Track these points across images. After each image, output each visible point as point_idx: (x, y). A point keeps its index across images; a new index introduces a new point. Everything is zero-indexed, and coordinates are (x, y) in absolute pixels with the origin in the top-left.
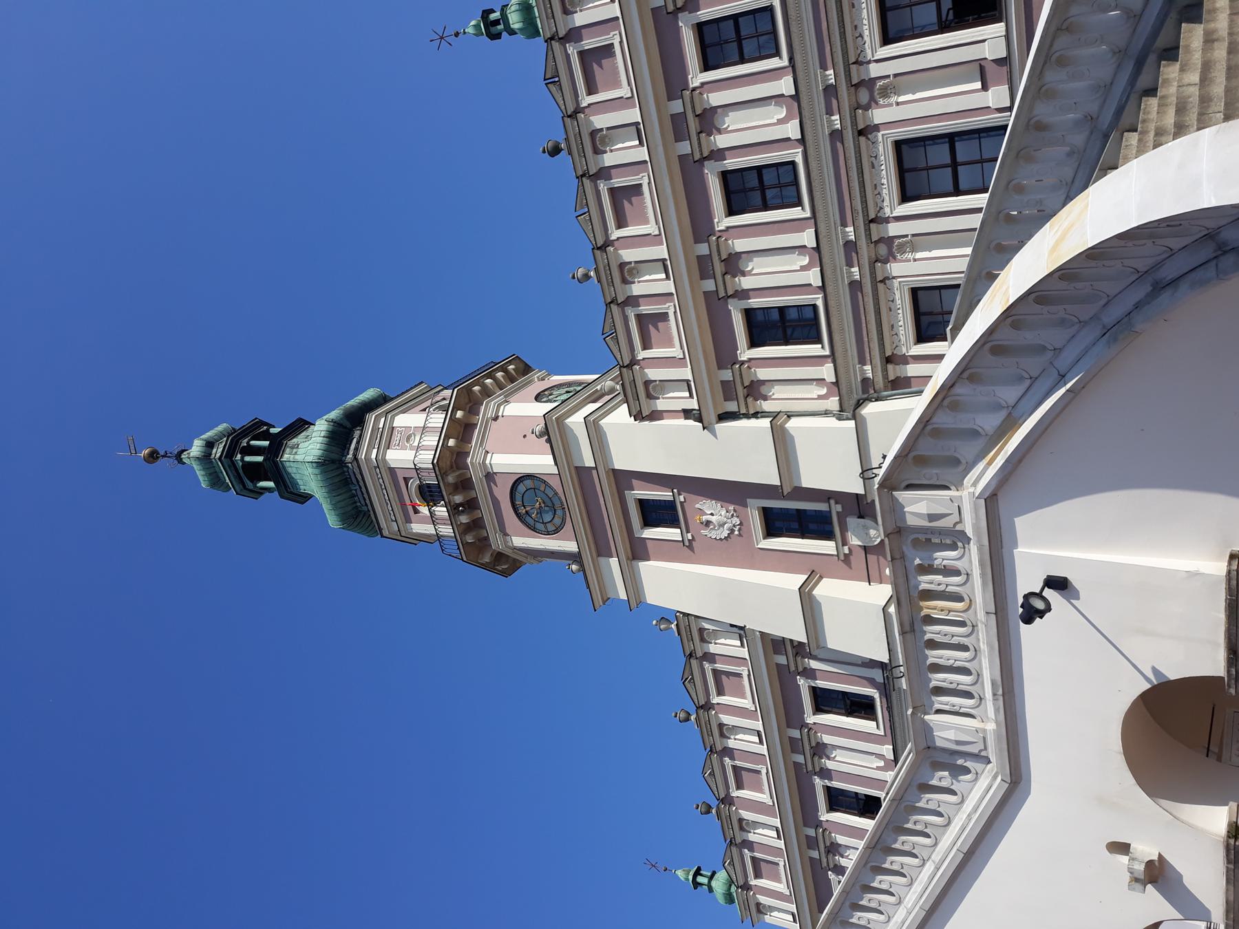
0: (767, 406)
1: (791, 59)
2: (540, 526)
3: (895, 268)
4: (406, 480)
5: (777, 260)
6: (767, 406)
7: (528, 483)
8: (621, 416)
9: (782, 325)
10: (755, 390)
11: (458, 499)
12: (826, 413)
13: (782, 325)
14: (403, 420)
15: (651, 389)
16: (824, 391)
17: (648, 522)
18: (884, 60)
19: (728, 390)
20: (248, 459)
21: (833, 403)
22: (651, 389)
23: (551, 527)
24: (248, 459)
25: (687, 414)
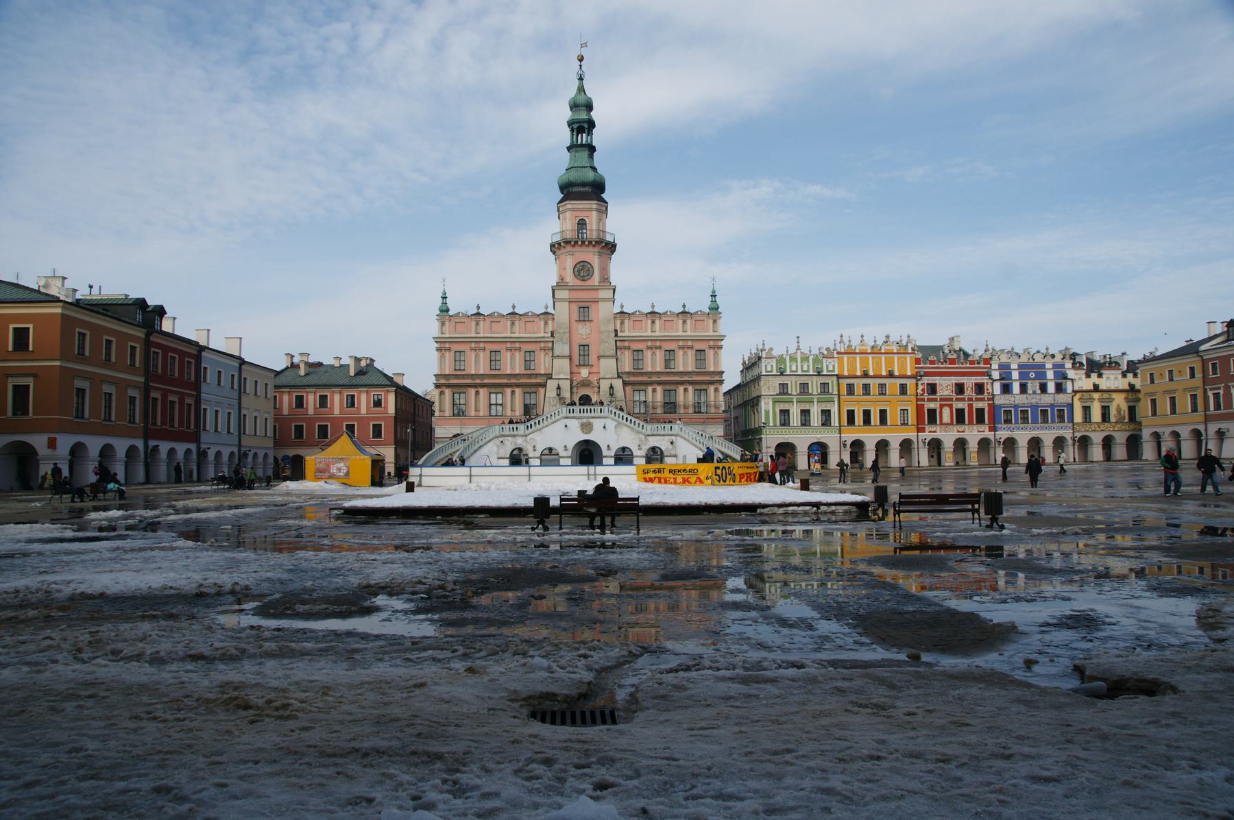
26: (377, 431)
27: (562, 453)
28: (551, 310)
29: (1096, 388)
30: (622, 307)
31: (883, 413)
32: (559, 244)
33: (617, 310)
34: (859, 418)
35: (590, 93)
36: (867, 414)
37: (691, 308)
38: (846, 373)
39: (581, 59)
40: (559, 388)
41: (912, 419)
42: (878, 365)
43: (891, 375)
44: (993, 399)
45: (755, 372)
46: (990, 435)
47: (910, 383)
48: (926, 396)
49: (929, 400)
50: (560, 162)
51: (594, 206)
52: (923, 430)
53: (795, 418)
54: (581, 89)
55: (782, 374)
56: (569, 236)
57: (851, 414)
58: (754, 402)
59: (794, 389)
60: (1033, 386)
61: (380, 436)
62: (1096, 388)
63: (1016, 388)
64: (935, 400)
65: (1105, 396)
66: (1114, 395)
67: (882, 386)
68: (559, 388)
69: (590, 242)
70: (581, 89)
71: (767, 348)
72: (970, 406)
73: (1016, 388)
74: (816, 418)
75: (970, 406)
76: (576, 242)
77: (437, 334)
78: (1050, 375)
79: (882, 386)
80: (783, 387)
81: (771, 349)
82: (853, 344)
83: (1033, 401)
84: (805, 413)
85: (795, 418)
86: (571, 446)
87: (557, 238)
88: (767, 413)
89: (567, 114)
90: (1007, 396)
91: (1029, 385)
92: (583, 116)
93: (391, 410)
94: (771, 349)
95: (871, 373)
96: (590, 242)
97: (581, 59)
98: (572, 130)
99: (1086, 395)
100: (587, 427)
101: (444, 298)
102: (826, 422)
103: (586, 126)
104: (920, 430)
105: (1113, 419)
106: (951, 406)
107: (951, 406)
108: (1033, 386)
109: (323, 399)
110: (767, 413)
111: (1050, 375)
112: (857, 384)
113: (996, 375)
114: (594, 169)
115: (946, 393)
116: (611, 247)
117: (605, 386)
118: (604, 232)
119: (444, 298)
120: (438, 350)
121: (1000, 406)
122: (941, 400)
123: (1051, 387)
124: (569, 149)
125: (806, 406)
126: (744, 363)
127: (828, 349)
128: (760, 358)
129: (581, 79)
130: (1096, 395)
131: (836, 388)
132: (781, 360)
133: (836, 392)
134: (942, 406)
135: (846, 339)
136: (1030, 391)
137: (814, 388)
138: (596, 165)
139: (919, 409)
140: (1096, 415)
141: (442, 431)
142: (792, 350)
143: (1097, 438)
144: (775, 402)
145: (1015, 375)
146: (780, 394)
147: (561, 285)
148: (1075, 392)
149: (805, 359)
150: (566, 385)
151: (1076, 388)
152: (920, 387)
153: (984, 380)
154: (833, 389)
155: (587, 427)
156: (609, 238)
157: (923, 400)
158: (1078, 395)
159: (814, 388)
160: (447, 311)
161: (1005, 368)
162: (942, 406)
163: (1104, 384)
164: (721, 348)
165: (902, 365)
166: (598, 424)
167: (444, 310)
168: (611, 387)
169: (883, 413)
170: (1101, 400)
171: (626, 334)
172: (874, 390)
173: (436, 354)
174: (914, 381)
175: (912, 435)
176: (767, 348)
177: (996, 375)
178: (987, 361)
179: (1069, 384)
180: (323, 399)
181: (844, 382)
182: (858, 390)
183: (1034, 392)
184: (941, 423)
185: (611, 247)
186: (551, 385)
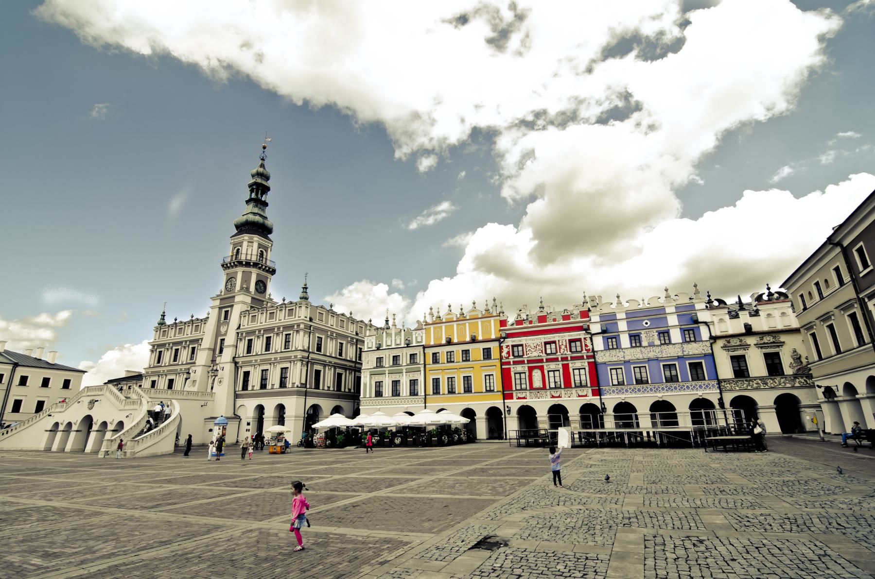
5: (258, 345)
8: (245, 308)
14: (255, 245)
29: (749, 331)
31: (467, 379)
34: (444, 387)
36: (451, 380)
38: (432, 343)
39: (264, 148)
41: (497, 384)
42: (461, 333)
43: (474, 340)
44: (594, 357)
46: (595, 401)
47: (494, 346)
48: (511, 359)
49: (515, 363)
52: (510, 397)
53: (387, 390)
54: (262, 166)
55: (378, 349)
57: (436, 382)
59: (387, 362)
60: (649, 337)
62: (749, 331)
63: (625, 341)
64: (522, 362)
65: (767, 339)
66: (783, 338)
67: (466, 352)
70: (262, 166)
72: (566, 368)
73: (625, 341)
74: (404, 389)
75: (566, 368)
78: (673, 320)
79: (466, 352)
80: (380, 360)
82: (441, 314)
83: (652, 355)
84: (396, 383)
85: (387, 390)
88: (365, 385)
90: (613, 352)
91: (643, 336)
95: (455, 340)
97: (264, 148)
99: (735, 342)
102: (413, 393)
104: (507, 396)
105: (788, 371)
106: (541, 368)
107: (541, 368)
108: (649, 337)
111: (673, 320)
112: (443, 351)
113: (595, 328)
115: (534, 354)
121: (605, 363)
122: (529, 362)
123: (676, 336)
125: (396, 377)
127: (418, 322)
130: (751, 341)
133: (422, 362)
134: (531, 369)
136: (645, 343)
137: (404, 360)
139: (506, 375)
140: (757, 365)
143: (765, 399)
145: (623, 326)
146: (377, 367)
148: (714, 339)
151: (716, 332)
152: (505, 350)
153: (581, 335)
154: (420, 359)
157: (509, 363)
158: (720, 343)
159: (404, 360)
161: (609, 320)
162: (531, 369)
163: (760, 324)
165: (486, 329)
169: (467, 379)
170: (759, 346)
172: (458, 356)
173: (150, 353)
174: (497, 344)
175: (498, 403)
177: (595, 328)
178: (585, 314)
179: (704, 330)
181: (430, 352)
182: (443, 358)
183: (651, 345)
184: (531, 388)
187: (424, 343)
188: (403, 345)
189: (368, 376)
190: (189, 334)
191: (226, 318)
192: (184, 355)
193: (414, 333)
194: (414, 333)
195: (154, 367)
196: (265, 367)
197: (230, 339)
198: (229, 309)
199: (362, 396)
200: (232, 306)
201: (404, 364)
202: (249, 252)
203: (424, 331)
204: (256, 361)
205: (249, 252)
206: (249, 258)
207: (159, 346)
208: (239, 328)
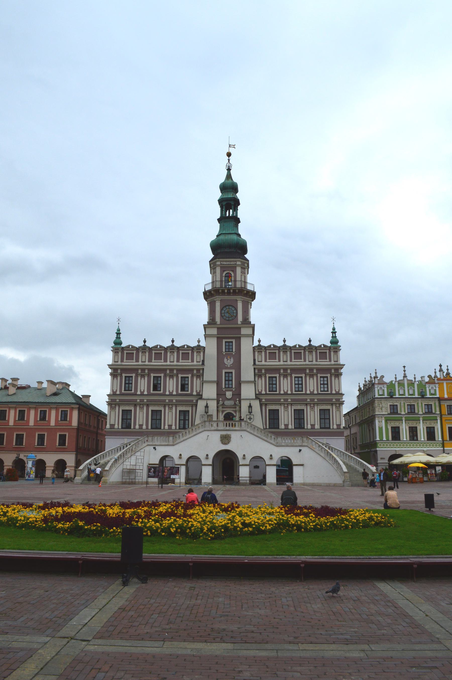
0: (257, 378)
1: (320, 394)
2: (223, 312)
3: (283, 407)
4: (233, 271)
5: (285, 385)
6: (257, 378)
7: (235, 312)
9: (272, 384)
10: (260, 376)
11: (232, 291)
12: (255, 391)
13: (272, 384)
15: (260, 352)
16: (260, 391)
17: (226, 342)
18: (317, 409)
19: (260, 370)
20: (233, 207)
21: (257, 393)
22: (260, 352)
23: (223, 315)
24: (233, 207)
25: (254, 360)
26: (62, 438)
27: (204, 462)
28: (203, 344)
30: (259, 341)
32: (210, 291)
33: (256, 343)
35: (235, 179)
37: (315, 343)
38: (446, 396)
39: (229, 155)
40: (207, 407)
45: (370, 396)
50: (213, 230)
51: (239, 263)
53: (405, 434)
54: (229, 176)
56: (218, 285)
58: (369, 422)
59: (403, 411)
61: (64, 444)
68: (207, 407)
69: (234, 291)
70: (229, 176)
71: (379, 375)
74: (422, 434)
76: (223, 291)
77: (111, 362)
81: (382, 377)
85: (405, 434)
86: (211, 456)
87: (209, 288)
88: (381, 429)
89: (218, 194)
92: (230, 195)
93: (75, 423)
94: (382, 377)
96: (234, 291)
97: (229, 155)
98: (222, 207)
100: (225, 439)
101: (118, 334)
103: (232, 203)
109: (22, 413)
110: (381, 429)
114: (239, 235)
116: (252, 295)
117: (244, 405)
118: (245, 282)
119: (118, 334)
120: (111, 374)
124: (219, 220)
125: (413, 424)
126: (360, 390)
127: (429, 376)
128: (373, 385)
129: (229, 170)
131: (438, 409)
132: (391, 385)
135: (444, 368)
137: (420, 409)
138: (240, 232)
141: (111, 443)
142: (400, 377)
144: (386, 421)
146: (391, 413)
147: (212, 322)
149: (411, 384)
150: (213, 405)
155: (225, 439)
156: (249, 287)
159: (420, 409)
160: (121, 343)
164: (341, 374)
166: (235, 436)
167: (118, 342)
168: (250, 406)
171: (263, 363)
173: (109, 378)
176: (379, 375)
180: (22, 413)
185: (252, 295)
186: (201, 404)
187: (438, 396)
188: (416, 396)
189: (383, 421)
190: (172, 361)
191: (229, 349)
192: (171, 385)
193: (427, 386)
194: (427, 386)
195: (121, 394)
196: (299, 407)
197: (247, 373)
198: (234, 341)
199: (378, 439)
200: (238, 339)
201: (421, 413)
202: (243, 280)
203: (437, 385)
204: (286, 400)
205: (243, 280)
206: (243, 286)
207: (124, 370)
208: (254, 364)
